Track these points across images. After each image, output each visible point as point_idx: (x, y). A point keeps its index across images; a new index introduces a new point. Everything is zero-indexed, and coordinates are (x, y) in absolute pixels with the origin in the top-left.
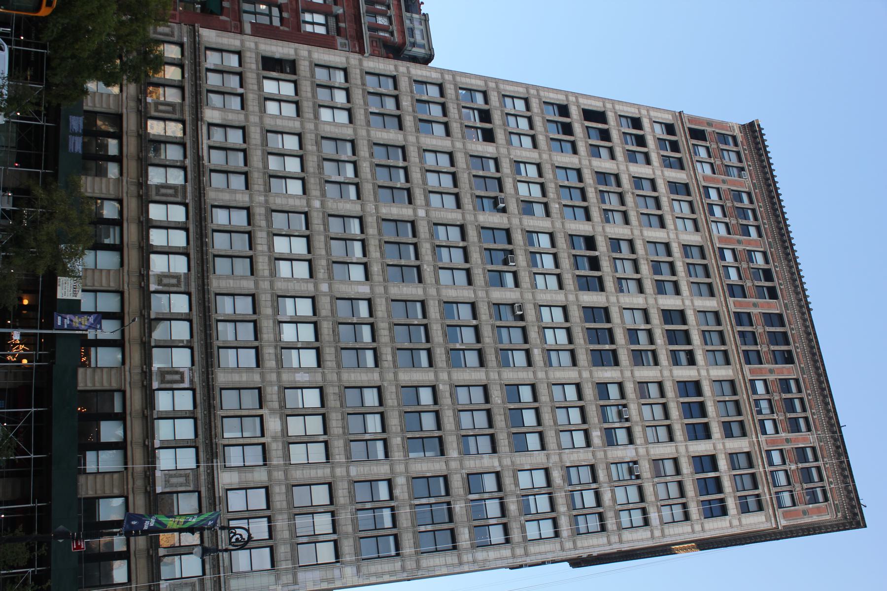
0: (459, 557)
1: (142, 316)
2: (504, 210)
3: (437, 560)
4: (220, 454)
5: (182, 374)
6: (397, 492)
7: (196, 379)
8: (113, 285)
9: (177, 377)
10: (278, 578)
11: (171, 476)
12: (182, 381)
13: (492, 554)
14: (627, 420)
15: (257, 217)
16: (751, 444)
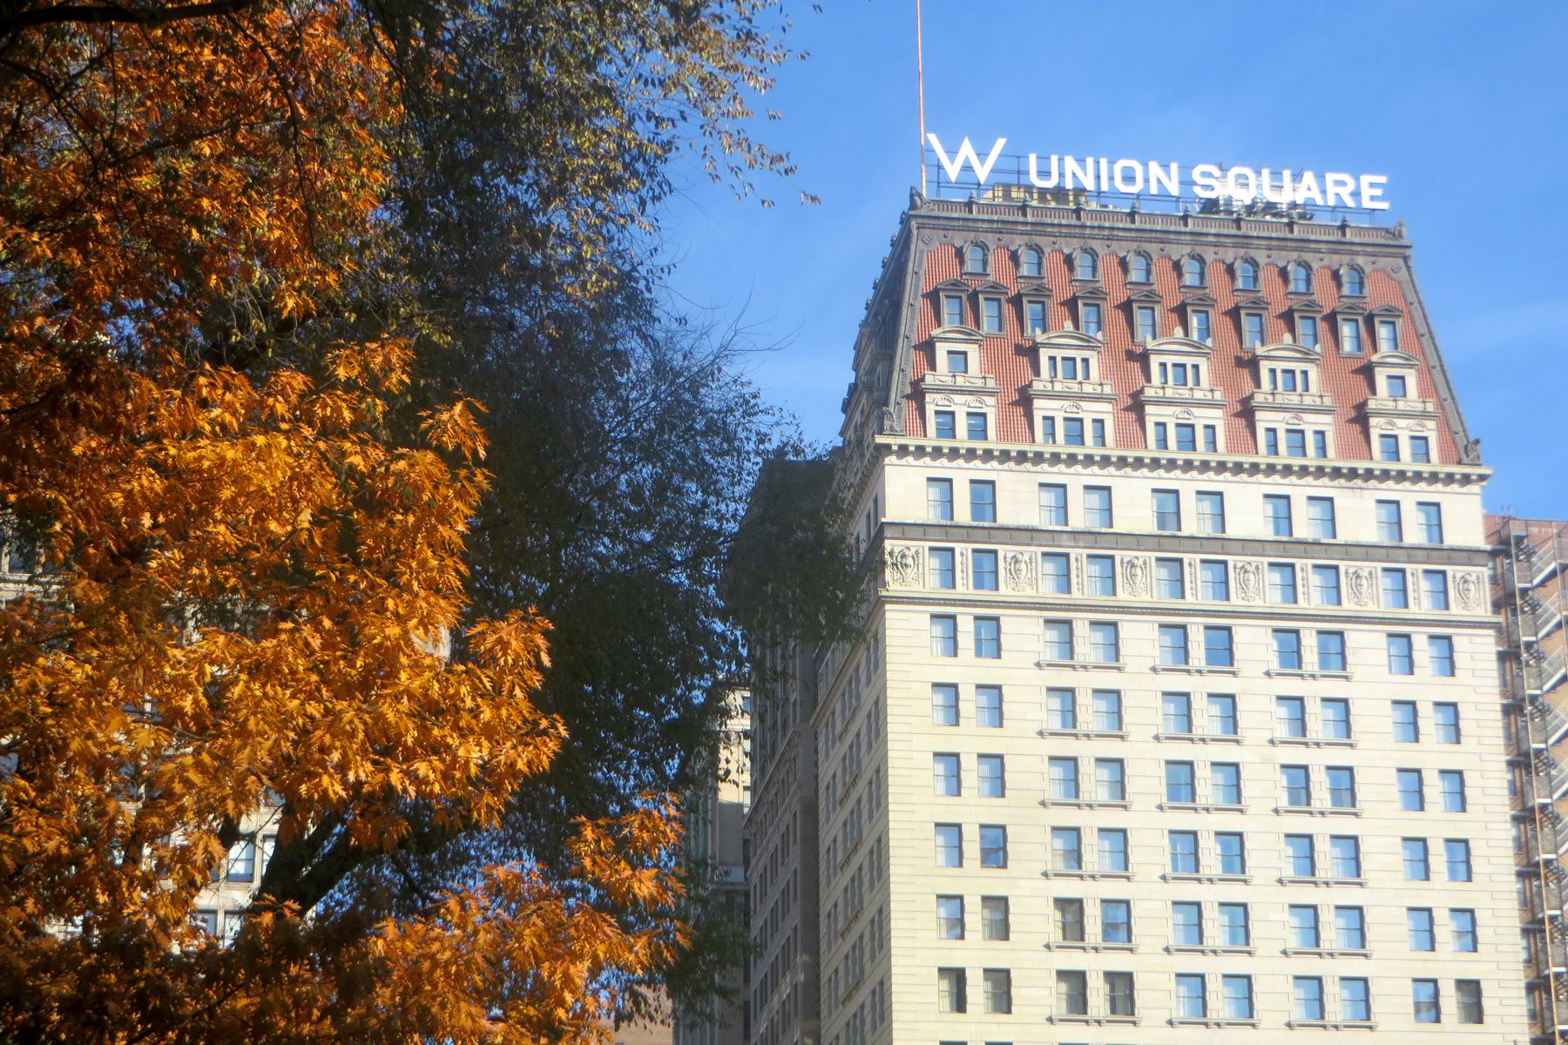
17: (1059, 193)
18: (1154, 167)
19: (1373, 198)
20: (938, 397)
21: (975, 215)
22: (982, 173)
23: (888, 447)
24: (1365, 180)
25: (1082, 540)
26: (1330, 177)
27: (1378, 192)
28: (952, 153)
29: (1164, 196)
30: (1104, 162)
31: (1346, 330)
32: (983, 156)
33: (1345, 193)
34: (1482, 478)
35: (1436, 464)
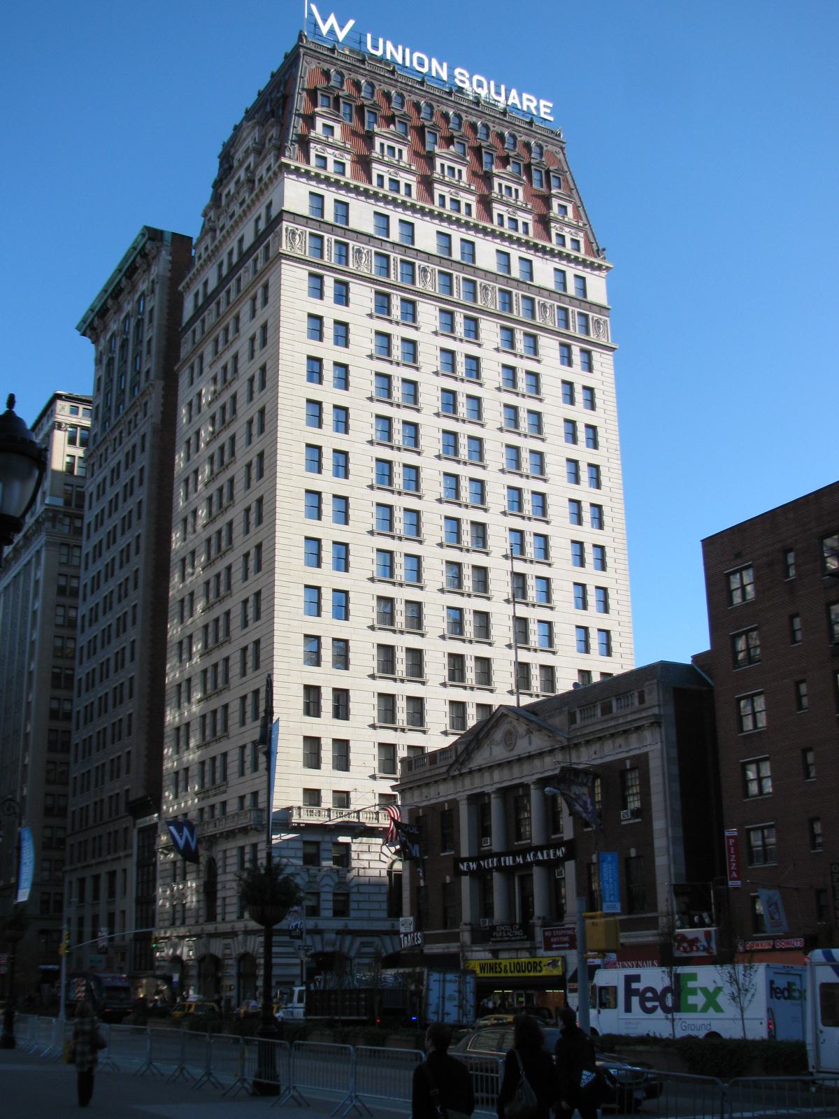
17: (381, 60)
18: (435, 62)
19: (545, 113)
20: (318, 147)
21: (335, 56)
22: (341, 35)
23: (288, 166)
24: (542, 103)
25: (398, 249)
26: (525, 96)
27: (548, 111)
28: (325, 21)
29: (439, 79)
30: (408, 51)
31: (535, 176)
32: (342, 27)
33: (533, 105)
34: (607, 268)
35: (582, 255)
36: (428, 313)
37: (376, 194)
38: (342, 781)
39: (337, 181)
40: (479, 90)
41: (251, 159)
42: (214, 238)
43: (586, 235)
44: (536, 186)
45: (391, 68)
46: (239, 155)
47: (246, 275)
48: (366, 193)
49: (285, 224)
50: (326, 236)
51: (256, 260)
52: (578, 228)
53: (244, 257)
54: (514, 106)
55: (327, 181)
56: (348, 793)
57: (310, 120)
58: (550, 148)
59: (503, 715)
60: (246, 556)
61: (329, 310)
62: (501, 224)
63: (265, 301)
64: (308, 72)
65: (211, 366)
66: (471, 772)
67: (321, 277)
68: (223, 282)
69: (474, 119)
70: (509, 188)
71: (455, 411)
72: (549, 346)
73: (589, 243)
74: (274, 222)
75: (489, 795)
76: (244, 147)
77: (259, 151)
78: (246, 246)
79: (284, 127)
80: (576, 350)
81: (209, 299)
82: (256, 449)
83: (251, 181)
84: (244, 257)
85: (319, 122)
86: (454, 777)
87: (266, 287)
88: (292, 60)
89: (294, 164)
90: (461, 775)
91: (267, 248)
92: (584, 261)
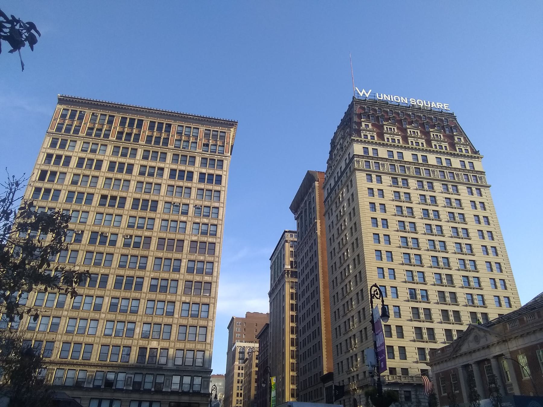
0: (214, 282)
1: (103, 392)
2: (83, 232)
3: (213, 290)
4: (162, 366)
5: (128, 377)
6: (187, 301)
7: (131, 372)
8: (88, 402)
9: (129, 379)
10: (208, 350)
11: (166, 385)
12: (131, 377)
13: (215, 270)
14: (180, 204)
15: (68, 339)
16: (199, 156)
22: (367, 96)
24: (445, 105)
28: (361, 92)
31: (447, 129)
32: (367, 93)
36: (413, 183)
37: (387, 144)
38: (404, 364)
39: (372, 142)
40: (420, 104)
41: (341, 141)
42: (331, 170)
43: (470, 147)
44: (447, 133)
45: (386, 103)
46: (337, 141)
47: (344, 179)
48: (383, 145)
49: (355, 159)
50: (371, 161)
51: (347, 173)
52: (467, 145)
53: (342, 173)
54: (434, 107)
55: (369, 142)
56: (407, 369)
57: (360, 124)
58: (450, 119)
59: (473, 329)
60: (353, 244)
61: (375, 186)
62: (436, 148)
63: (352, 186)
64: (357, 109)
65: (335, 212)
66: (461, 355)
67: (371, 175)
68: (336, 183)
69: (420, 114)
70: (437, 135)
71: (429, 216)
72: (463, 189)
73: (471, 149)
74: (351, 160)
75: (471, 365)
76: (338, 138)
77: (344, 138)
78: (342, 170)
79: (351, 128)
80: (474, 189)
81: (332, 190)
82: (355, 237)
83: (342, 148)
84: (342, 173)
85: (363, 124)
86: (453, 358)
87: (351, 181)
88: (351, 107)
89: (356, 139)
90: (457, 357)
91: (350, 168)
92: (471, 156)
